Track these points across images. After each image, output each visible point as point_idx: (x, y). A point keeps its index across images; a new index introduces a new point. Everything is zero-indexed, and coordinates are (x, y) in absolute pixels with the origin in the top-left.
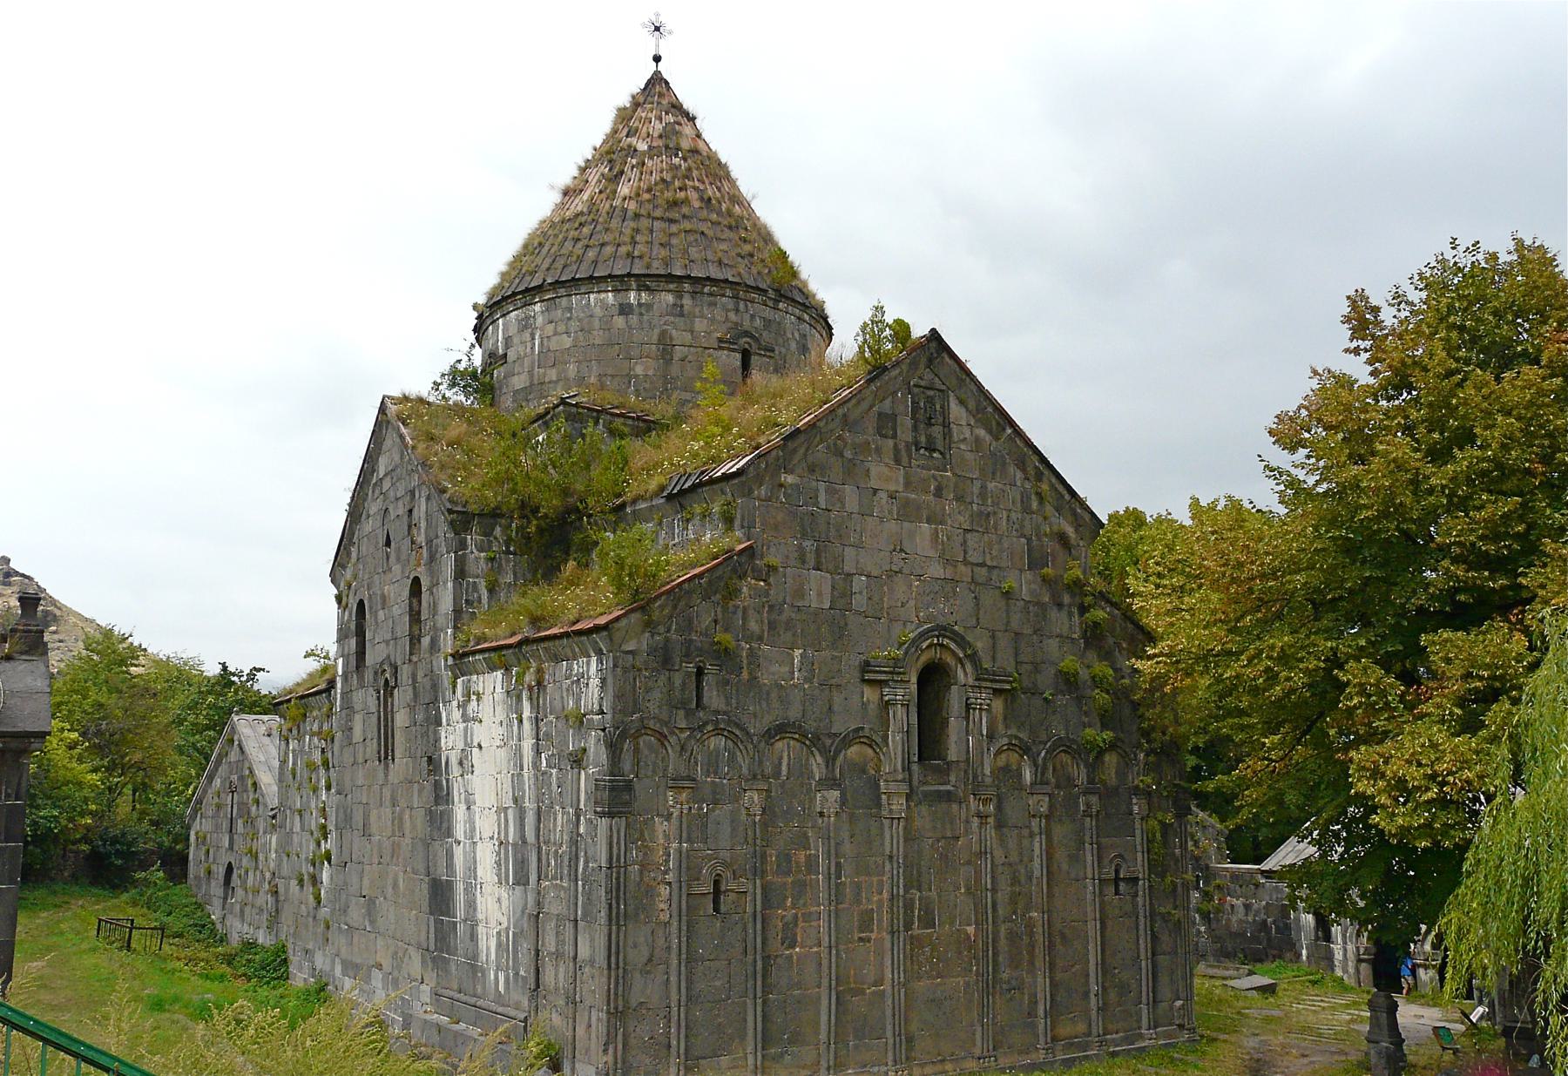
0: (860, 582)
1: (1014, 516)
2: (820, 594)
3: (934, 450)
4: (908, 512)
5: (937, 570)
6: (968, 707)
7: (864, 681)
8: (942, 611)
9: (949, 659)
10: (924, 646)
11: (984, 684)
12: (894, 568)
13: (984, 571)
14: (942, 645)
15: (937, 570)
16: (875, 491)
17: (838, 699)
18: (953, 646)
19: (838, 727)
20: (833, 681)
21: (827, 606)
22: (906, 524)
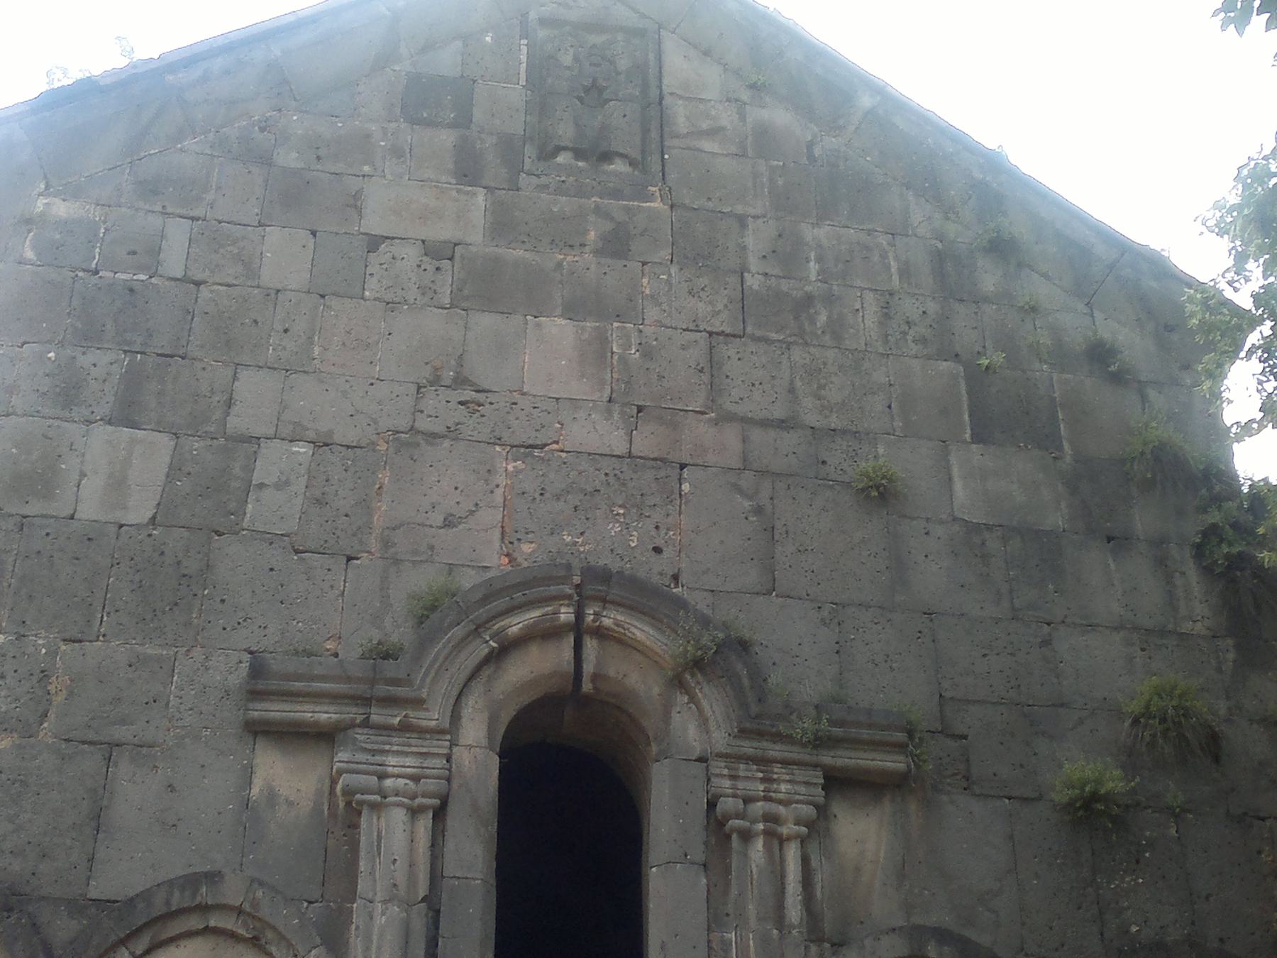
0: (275, 461)
1: (908, 307)
2: (118, 485)
3: (606, 157)
4: (487, 288)
5: (598, 433)
6: (719, 832)
7: (259, 731)
8: (611, 539)
9: (641, 683)
10: (515, 625)
11: (775, 750)
12: (423, 424)
13: (789, 440)
14: (601, 634)
15: (598, 433)
16: (374, 243)
17: (134, 792)
18: (641, 631)
19: (124, 872)
20: (121, 733)
21: (139, 510)
22: (485, 322)
